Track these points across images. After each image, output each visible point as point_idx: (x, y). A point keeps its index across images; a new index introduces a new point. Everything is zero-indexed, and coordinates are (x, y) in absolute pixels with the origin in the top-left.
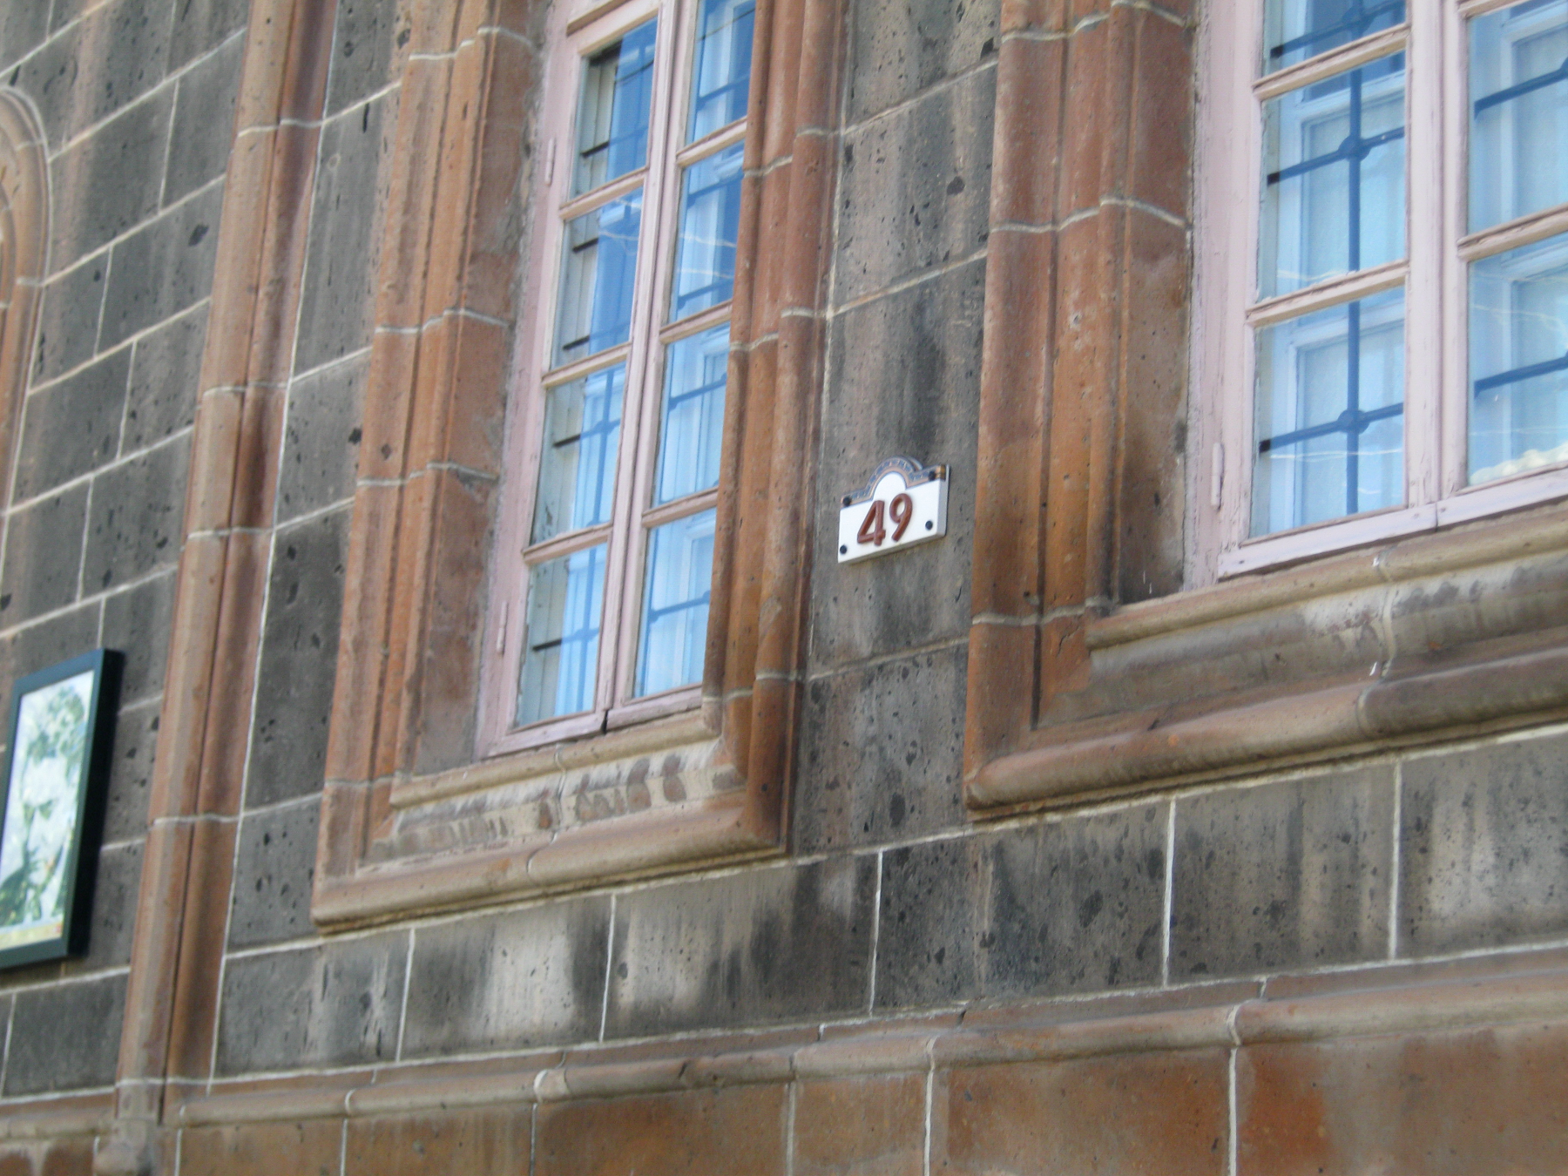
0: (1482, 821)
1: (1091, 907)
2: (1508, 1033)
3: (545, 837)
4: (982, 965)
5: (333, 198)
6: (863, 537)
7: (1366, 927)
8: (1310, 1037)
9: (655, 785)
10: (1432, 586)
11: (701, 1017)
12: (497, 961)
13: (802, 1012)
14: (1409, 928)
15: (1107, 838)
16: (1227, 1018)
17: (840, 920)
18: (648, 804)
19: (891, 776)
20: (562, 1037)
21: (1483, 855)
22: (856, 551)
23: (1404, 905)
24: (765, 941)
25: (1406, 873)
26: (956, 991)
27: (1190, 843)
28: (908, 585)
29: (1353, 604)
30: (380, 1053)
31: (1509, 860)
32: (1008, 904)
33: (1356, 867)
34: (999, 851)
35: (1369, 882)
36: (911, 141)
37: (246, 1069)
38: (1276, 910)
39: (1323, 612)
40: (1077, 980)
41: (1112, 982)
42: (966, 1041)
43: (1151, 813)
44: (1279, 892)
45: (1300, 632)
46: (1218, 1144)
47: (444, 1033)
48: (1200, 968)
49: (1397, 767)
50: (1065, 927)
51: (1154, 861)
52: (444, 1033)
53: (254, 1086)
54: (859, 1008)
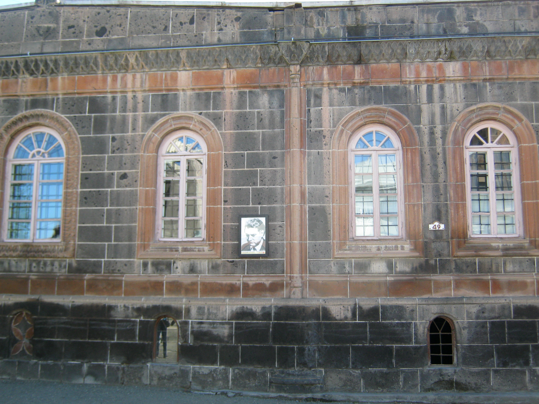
0: (511, 263)
1: (468, 267)
2: (518, 280)
3: (379, 252)
4: (454, 270)
5: (313, 162)
6: (433, 228)
7: (500, 271)
8: (497, 279)
9: (399, 249)
10: (505, 244)
11: (411, 272)
12: (372, 264)
13: (429, 273)
14: (505, 271)
15: (469, 261)
16: (489, 277)
17: (432, 265)
18: (398, 250)
19: (439, 252)
20: (386, 274)
21: (511, 266)
22: (432, 229)
23: (504, 269)
24: (421, 266)
25: (504, 267)
26: (450, 273)
27: (479, 262)
28: (439, 233)
29: (497, 244)
30: (349, 273)
31: (514, 267)
32: (456, 265)
33: (498, 266)
34: (455, 260)
35: (500, 267)
36: (433, 188)
37: (317, 274)
38: (490, 269)
39: (493, 244)
40: (466, 273)
41: (471, 273)
42: (457, 278)
43: (474, 259)
44: (490, 267)
45: (491, 246)
46: (489, 288)
47: (363, 272)
48: (482, 273)
49: (502, 258)
50: (465, 268)
51: (475, 263)
52: (363, 272)
53: (320, 276)
54: (437, 273)
